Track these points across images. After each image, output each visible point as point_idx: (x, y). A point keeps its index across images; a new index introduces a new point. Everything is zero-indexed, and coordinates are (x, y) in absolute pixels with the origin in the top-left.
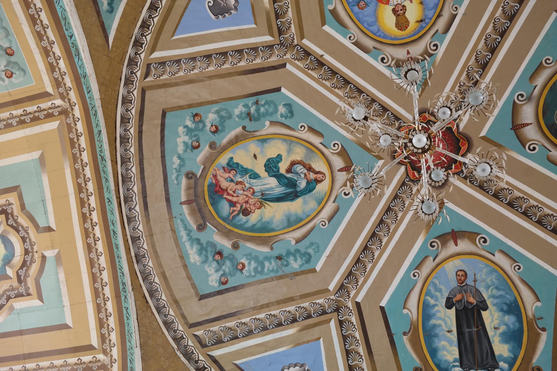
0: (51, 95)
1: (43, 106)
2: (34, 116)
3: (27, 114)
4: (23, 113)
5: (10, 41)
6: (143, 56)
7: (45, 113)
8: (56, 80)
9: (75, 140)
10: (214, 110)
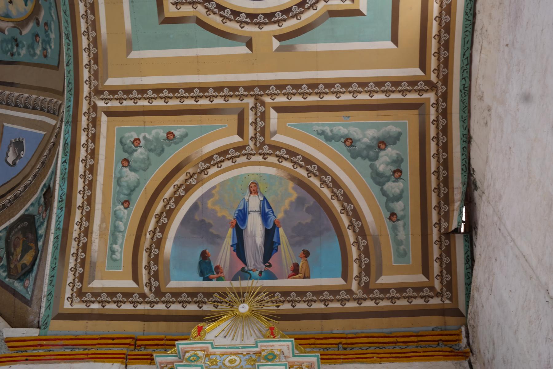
0: (105, 112)
1: (116, 103)
2: (128, 96)
3: (135, 99)
4: (138, 101)
7: (116, 96)
8: (94, 126)
9: (92, 62)
10: (36, 58)
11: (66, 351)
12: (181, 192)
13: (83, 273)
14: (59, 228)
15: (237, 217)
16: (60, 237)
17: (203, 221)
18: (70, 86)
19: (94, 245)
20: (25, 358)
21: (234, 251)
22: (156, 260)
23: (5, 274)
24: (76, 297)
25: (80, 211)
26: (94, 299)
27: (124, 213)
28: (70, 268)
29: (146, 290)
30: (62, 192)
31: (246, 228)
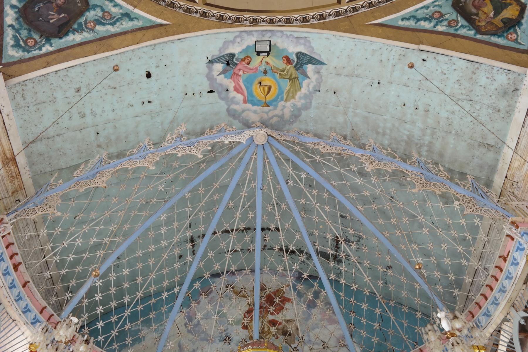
23: (472, 33)
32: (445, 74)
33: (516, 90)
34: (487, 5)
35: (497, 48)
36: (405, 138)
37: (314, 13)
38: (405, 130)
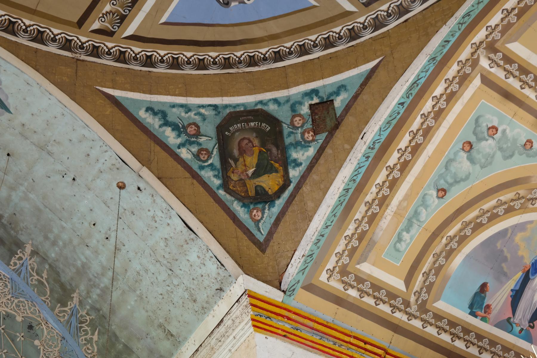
0: (482, 76)
1: (501, 74)
2: (520, 75)
3: (525, 83)
4: (527, 87)
5: (456, 154)
6: (362, 20)
7: (507, 66)
8: (460, 84)
9: (516, 11)
11: (315, 336)
12: (501, 210)
13: (357, 247)
14: (354, 180)
15: (533, 264)
16: (351, 192)
17: (502, 251)
18: (467, 18)
19: (384, 220)
20: (284, 333)
21: (511, 296)
22: (438, 270)
23: (217, 182)
24: (337, 273)
25: (388, 173)
26: (355, 284)
27: (434, 202)
28: (345, 235)
29: (413, 299)
30: (379, 138)
31: (534, 279)
32: (156, 222)
33: (221, 289)
34: (253, 154)
35: (231, 221)
36: (79, 263)
37: (32, 23)
38: (83, 254)
